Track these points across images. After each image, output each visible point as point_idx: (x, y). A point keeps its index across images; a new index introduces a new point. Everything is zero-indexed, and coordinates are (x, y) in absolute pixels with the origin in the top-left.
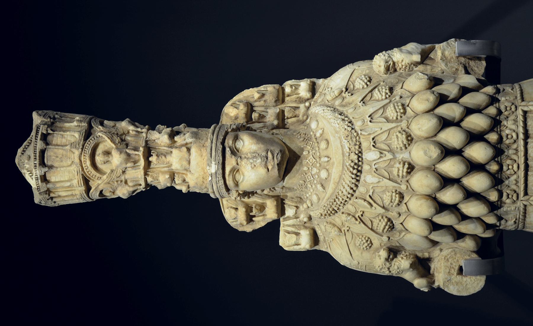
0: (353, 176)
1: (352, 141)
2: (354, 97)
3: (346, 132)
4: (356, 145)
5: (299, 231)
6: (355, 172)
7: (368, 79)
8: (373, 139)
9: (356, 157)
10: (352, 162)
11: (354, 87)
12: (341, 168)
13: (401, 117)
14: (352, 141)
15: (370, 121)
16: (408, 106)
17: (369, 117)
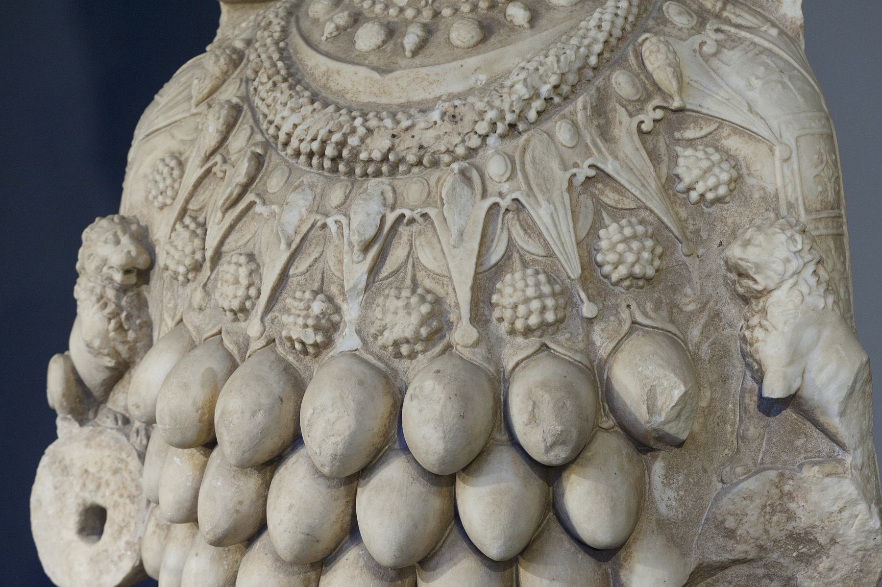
0: (315, 146)
2: (628, 144)
6: (330, 151)
7: (710, 196)
8: (424, 215)
9: (377, 155)
10: (362, 140)
11: (691, 143)
12: (364, 98)
14: (438, 138)
15: (496, 204)
16: (544, 347)
17: (516, 200)
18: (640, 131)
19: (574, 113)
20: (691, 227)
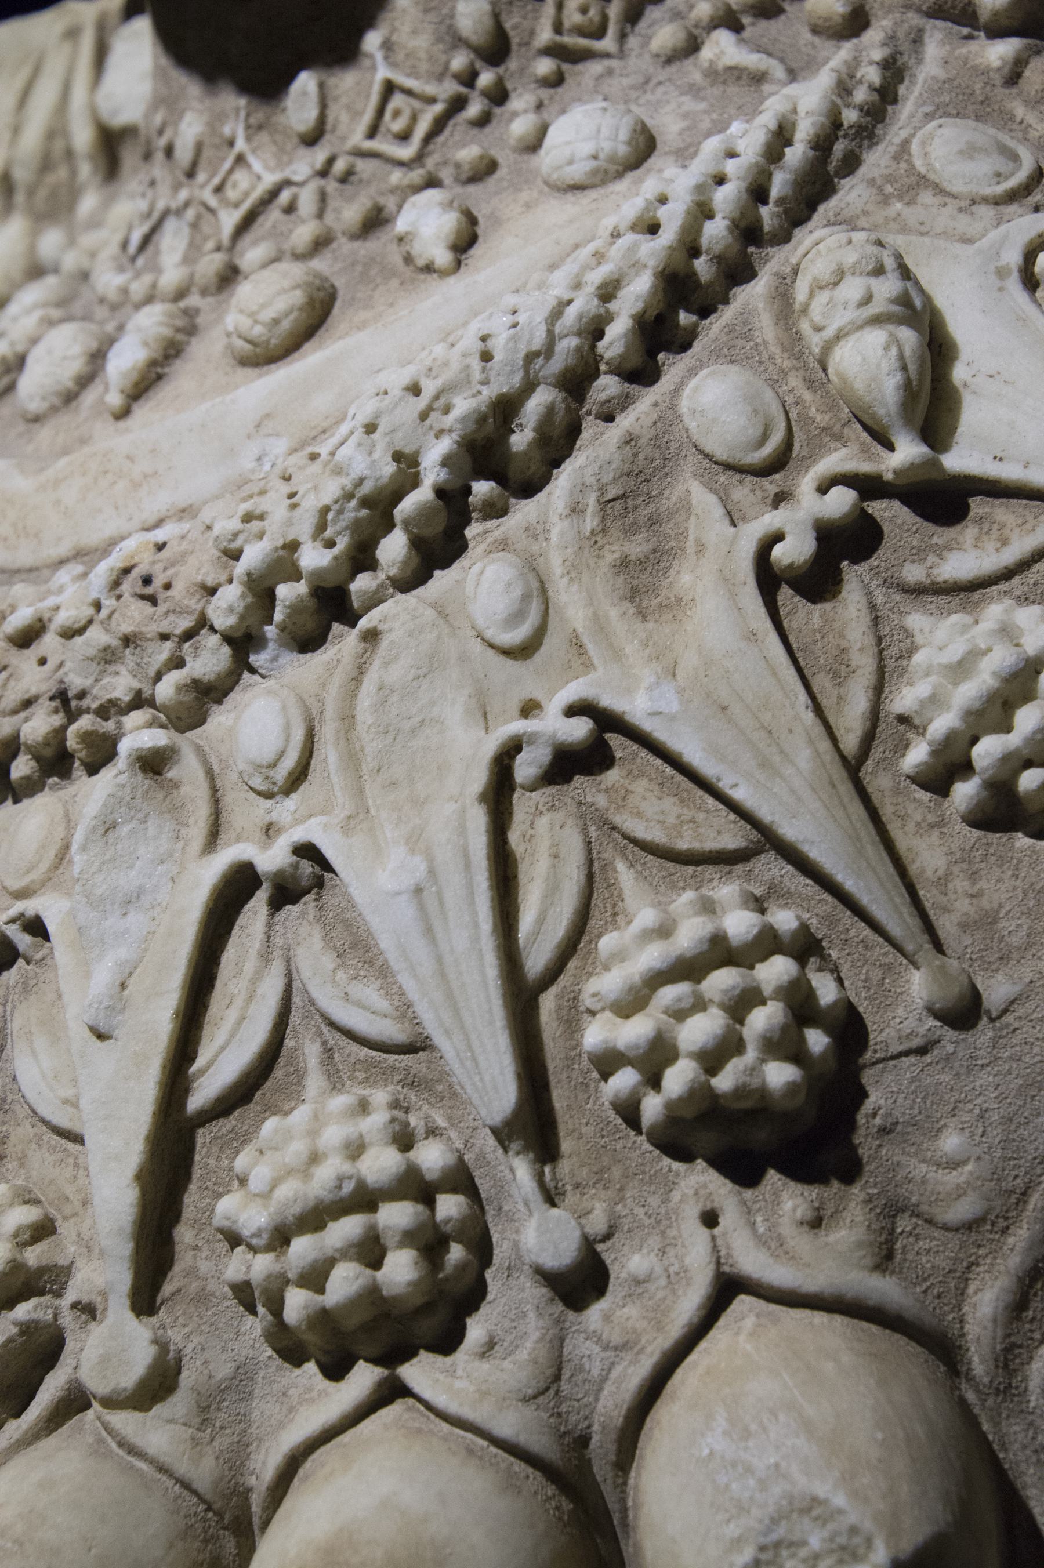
1: (108, 657)
3: (202, 566)
4: (65, 701)
5: (20, 198)
13: (244, 1294)
14: (108, 657)
17: (307, 851)
18: (768, 578)
19: (535, 532)
20: (963, 905)
